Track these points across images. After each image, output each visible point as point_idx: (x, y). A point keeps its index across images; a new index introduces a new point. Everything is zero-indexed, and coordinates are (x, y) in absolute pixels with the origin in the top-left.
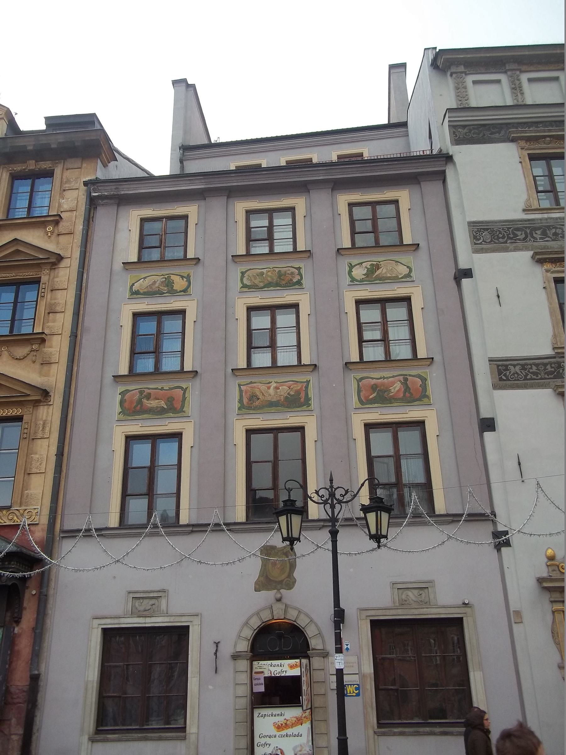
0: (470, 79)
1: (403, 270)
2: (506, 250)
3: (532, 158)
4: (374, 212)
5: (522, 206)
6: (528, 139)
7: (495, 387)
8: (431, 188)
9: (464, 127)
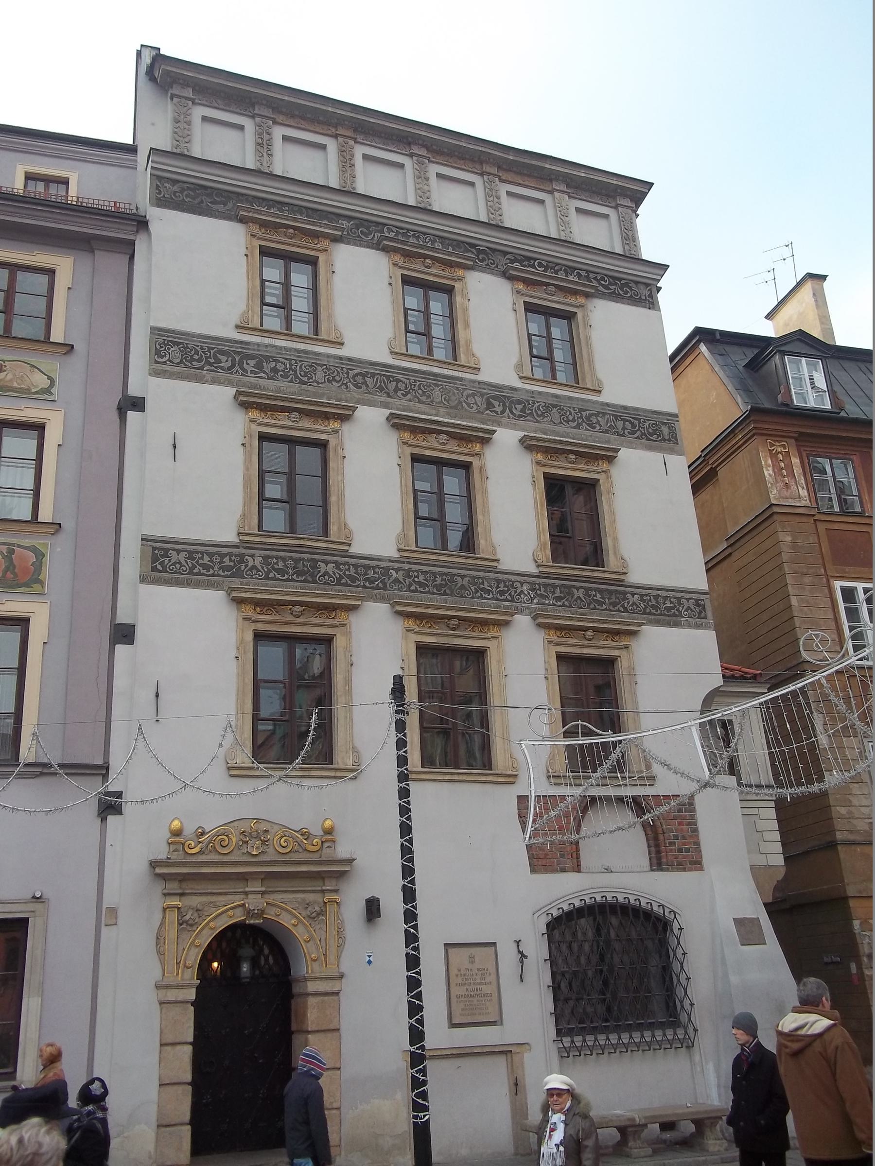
0: (199, 112)
1: (41, 381)
2: (200, 380)
3: (265, 252)
4: (12, 280)
5: (236, 319)
6: (264, 224)
7: (144, 579)
8: (110, 263)
9: (175, 182)
